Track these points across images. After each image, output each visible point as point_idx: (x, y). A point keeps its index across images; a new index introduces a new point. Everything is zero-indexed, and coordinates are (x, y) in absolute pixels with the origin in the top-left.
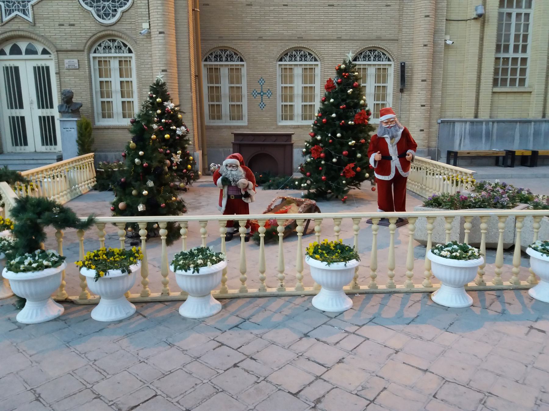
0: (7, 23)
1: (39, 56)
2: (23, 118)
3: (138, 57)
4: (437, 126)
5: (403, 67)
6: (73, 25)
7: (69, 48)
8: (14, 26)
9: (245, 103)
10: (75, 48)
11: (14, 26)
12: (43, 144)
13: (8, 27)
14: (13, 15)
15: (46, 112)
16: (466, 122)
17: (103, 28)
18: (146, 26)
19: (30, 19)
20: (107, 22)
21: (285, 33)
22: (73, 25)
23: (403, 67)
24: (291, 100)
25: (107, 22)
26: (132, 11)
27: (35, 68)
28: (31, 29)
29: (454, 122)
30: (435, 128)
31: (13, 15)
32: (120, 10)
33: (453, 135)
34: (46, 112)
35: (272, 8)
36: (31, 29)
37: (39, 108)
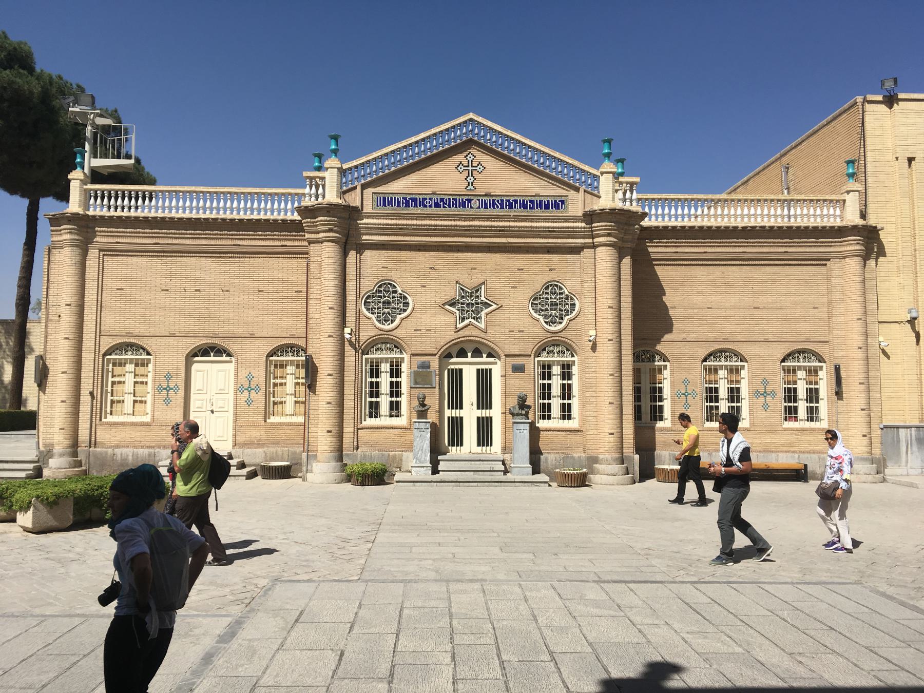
0: (462, 329)
1: (485, 359)
2: (461, 418)
3: (582, 362)
4: (879, 431)
5: (837, 370)
6: (522, 331)
7: (517, 353)
8: (466, 332)
9: (745, 405)
10: (523, 353)
11: (466, 332)
12: (479, 445)
13: (461, 333)
14: (467, 322)
15: (484, 413)
16: (910, 427)
17: (549, 335)
18: (593, 333)
19: (482, 326)
20: (553, 328)
21: (710, 335)
22: (522, 331)
23: (837, 370)
24: (817, 402)
25: (553, 328)
26: (578, 320)
27: (478, 370)
28: (482, 335)
29: (898, 427)
30: (876, 434)
31: (467, 322)
32: (566, 318)
33: (899, 441)
34: (484, 413)
35: (696, 311)
36: (482, 335)
37: (478, 408)
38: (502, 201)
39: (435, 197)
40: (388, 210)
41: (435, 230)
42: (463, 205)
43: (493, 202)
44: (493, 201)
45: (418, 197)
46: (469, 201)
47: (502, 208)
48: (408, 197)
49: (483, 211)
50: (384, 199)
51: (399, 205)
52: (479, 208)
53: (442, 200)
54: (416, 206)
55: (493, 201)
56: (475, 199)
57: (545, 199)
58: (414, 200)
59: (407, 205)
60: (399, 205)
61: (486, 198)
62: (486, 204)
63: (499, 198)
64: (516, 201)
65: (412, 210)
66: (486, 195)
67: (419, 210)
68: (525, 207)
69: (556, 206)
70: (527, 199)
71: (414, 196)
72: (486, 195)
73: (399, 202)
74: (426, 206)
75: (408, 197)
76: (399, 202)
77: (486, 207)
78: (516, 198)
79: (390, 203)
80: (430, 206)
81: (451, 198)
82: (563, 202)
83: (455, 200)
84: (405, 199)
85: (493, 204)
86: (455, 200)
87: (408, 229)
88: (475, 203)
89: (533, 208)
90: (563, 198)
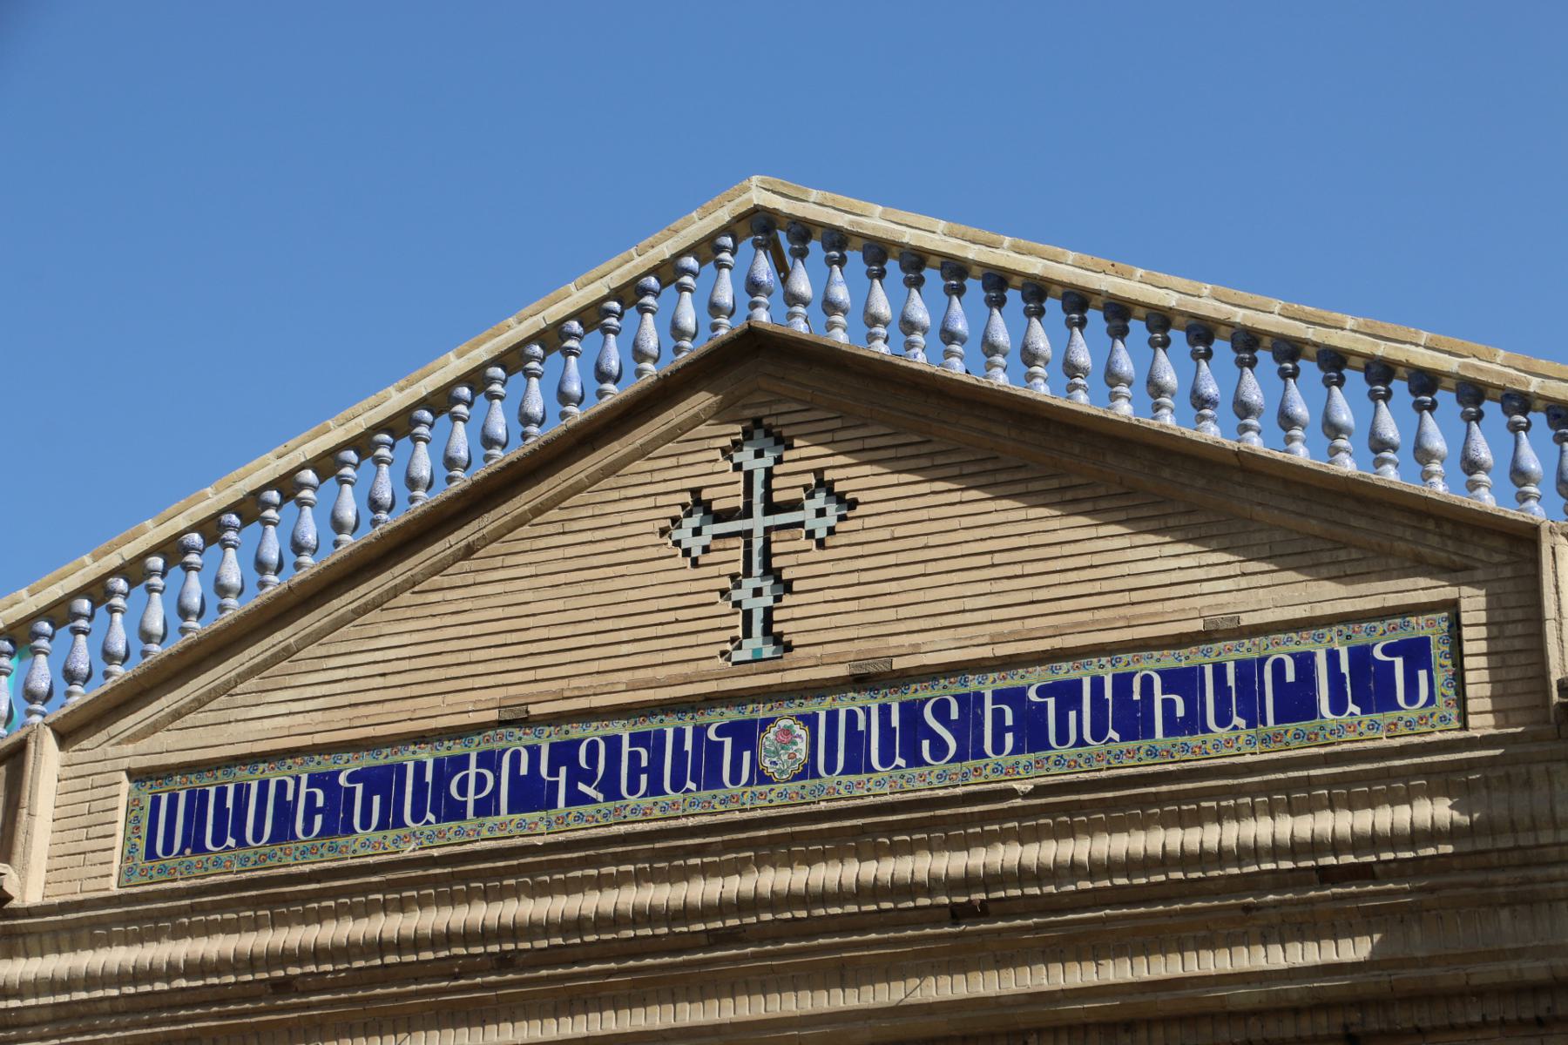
38: (970, 703)
39: (518, 741)
40: (224, 865)
41: (504, 962)
42: (704, 767)
43: (911, 709)
44: (911, 712)
45: (408, 757)
46: (745, 735)
47: (970, 749)
48: (346, 767)
49: (839, 788)
50: (197, 800)
51: (283, 832)
52: (808, 771)
53: (563, 753)
54: (392, 819)
55: (911, 712)
56: (786, 716)
57: (1283, 649)
58: (382, 781)
59: (337, 821)
60: (283, 832)
61: (843, 705)
62: (857, 740)
63: (948, 689)
64: (1067, 694)
65: (366, 844)
66: (860, 682)
67: (419, 838)
68: (1134, 722)
69: (1369, 684)
70: (1149, 665)
71: (383, 758)
72: (860, 682)
73: (285, 812)
74: (455, 812)
75: (346, 767)
76: (285, 812)
77: (857, 763)
78: (1065, 672)
79: (231, 824)
80: (486, 807)
81: (623, 730)
82: (1416, 653)
83: (654, 742)
84: (325, 781)
85: (909, 738)
86: (654, 742)
87: (320, 983)
88: (786, 743)
89: (1193, 723)
90: (1419, 627)
